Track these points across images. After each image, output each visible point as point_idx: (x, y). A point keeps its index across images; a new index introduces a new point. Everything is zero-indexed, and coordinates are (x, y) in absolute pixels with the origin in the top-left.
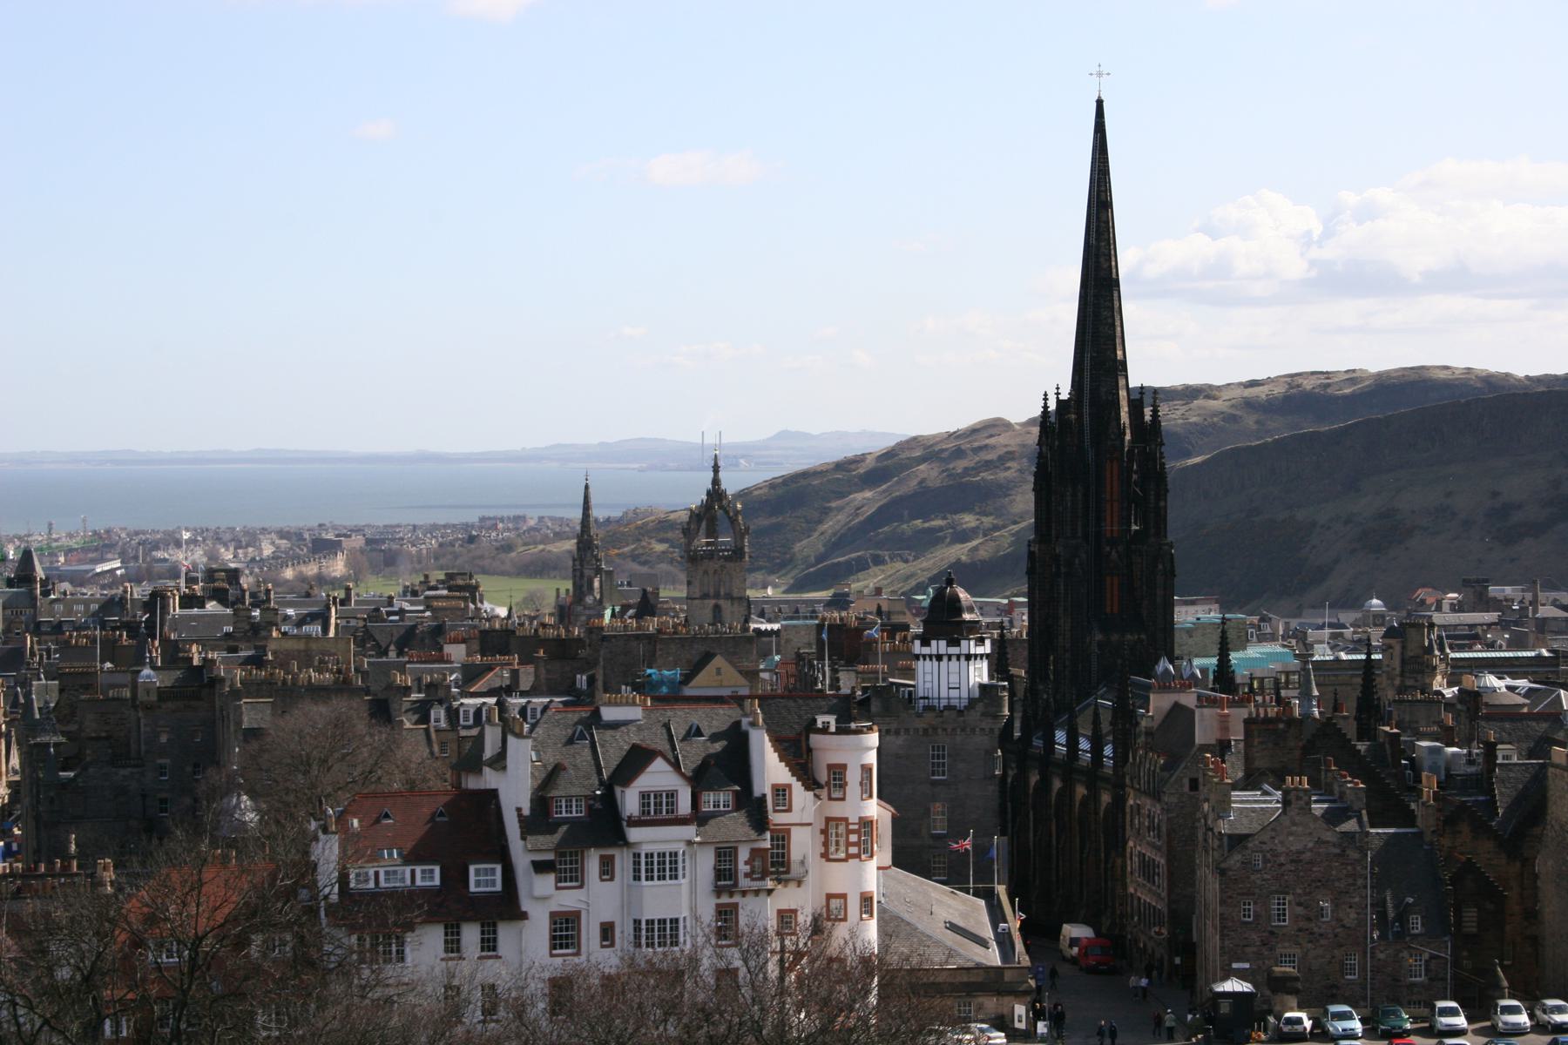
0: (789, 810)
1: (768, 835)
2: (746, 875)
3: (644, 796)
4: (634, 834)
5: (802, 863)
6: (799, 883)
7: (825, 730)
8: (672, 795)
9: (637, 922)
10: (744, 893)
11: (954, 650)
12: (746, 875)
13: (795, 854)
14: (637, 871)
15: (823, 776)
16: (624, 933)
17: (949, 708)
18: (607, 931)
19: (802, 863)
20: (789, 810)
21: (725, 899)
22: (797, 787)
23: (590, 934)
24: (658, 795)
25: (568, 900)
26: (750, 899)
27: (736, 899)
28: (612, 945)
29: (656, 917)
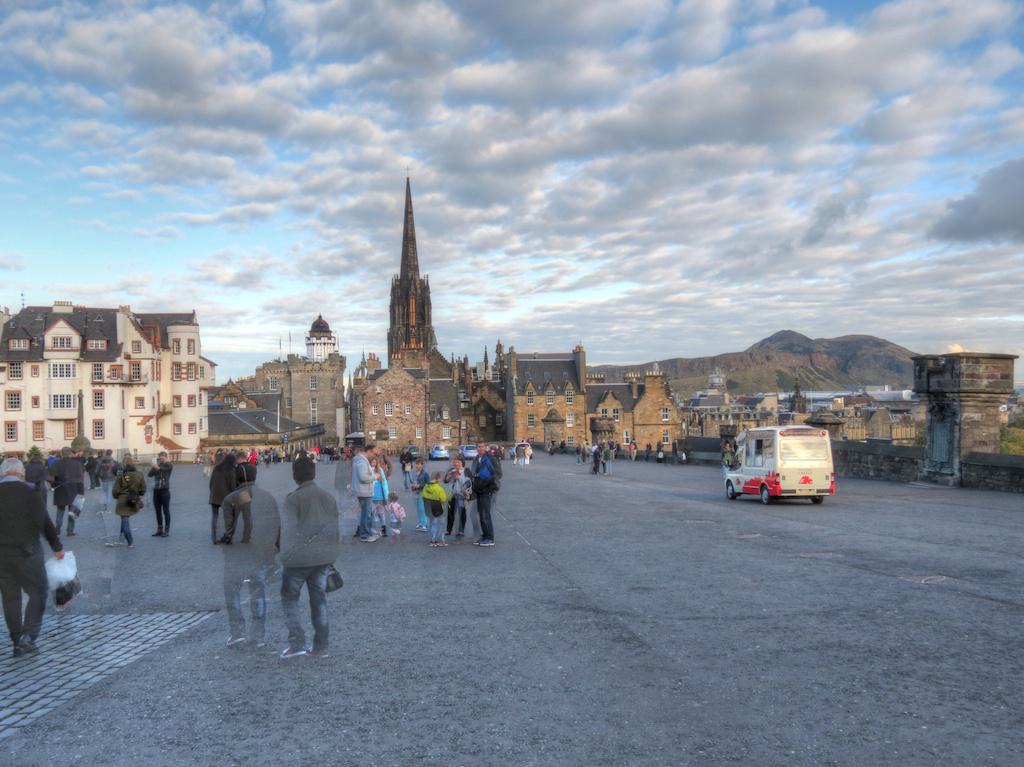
3: (55, 339)
4: (46, 355)
8: (69, 339)
11: (318, 341)
15: (171, 344)
17: (317, 363)
18: (36, 401)
21: (97, 387)
23: (26, 400)
27: (103, 387)
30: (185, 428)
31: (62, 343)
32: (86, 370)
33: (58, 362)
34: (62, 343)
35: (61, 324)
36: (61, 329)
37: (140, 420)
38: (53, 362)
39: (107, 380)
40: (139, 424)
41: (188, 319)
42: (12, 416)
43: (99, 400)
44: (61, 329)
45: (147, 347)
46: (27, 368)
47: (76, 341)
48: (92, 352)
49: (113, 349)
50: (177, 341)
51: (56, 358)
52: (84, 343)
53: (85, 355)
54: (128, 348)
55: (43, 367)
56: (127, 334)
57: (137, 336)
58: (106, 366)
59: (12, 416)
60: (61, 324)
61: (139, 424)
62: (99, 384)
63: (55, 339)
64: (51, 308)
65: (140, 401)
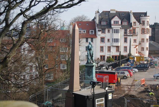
0: (136, 25)
1: (132, 28)
2: (129, 33)
3: (114, 22)
4: (112, 26)
5: (137, 33)
6: (137, 35)
7: (142, 16)
8: (118, 22)
9: (113, 39)
10: (128, 36)
12: (129, 33)
13: (136, 32)
14: (113, 32)
15: (141, 22)
16: (111, 40)
18: (109, 40)
19: (137, 33)
20: (136, 25)
21: (125, 37)
22: (137, 22)
23: (106, 40)
24: (116, 21)
25: (103, 35)
26: (129, 36)
27: (127, 36)
28: (109, 42)
29: (115, 38)
30: (145, 49)
31: (116, 23)
35: (116, 17)
36: (116, 19)
37: (135, 46)
38: (114, 29)
39: (128, 34)
40: (134, 48)
41: (145, 14)
44: (116, 19)
45: (137, 23)
46: (107, 30)
47: (120, 23)
48: (124, 26)
49: (130, 25)
50: (144, 22)
53: (123, 27)
54: (133, 25)
55: (111, 30)
56: (133, 20)
57: (135, 20)
58: (128, 30)
59: (102, 44)
60: (116, 17)
61: (134, 48)
62: (126, 36)
64: (109, 12)
65: (135, 41)
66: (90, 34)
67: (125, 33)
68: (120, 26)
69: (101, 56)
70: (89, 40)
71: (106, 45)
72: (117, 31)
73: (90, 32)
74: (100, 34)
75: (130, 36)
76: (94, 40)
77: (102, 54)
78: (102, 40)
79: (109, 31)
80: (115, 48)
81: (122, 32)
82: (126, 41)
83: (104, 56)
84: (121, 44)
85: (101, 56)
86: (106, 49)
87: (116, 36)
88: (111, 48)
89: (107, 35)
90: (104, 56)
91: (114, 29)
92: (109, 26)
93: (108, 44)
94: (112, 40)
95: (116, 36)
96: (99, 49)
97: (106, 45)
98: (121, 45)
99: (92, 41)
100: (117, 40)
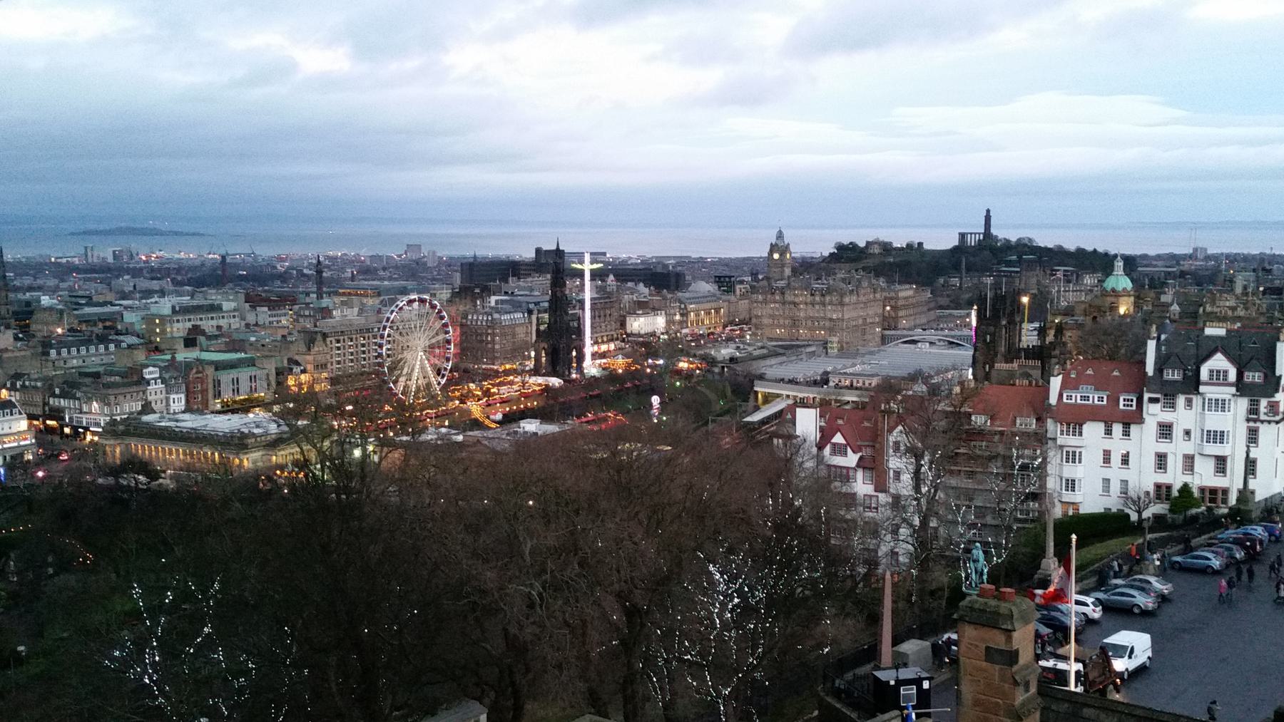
3: (1211, 371)
4: (1202, 389)
8: (1226, 372)
10: (1262, 422)
18: (1188, 433)
21: (1252, 424)
23: (1178, 432)
24: (1218, 372)
25: (1167, 417)
27: (1258, 424)
31: (1218, 378)
32: (1243, 404)
33: (1214, 396)
34: (1218, 378)
35: (1219, 356)
36: (1219, 362)
38: (1208, 396)
39: (1263, 417)
42: (1163, 447)
43: (1253, 436)
44: (1219, 362)
46: (1181, 400)
47: (1232, 376)
51: (1208, 391)
52: (1240, 375)
53: (1242, 388)
55: (1197, 401)
58: (1264, 403)
59: (1163, 447)
60: (1219, 356)
62: (1255, 421)
63: (1211, 371)
66: (1121, 407)
67: (1253, 410)
68: (1233, 390)
69: (1158, 487)
70: (1117, 429)
71: (1177, 449)
72: (1221, 405)
73: (1122, 402)
74: (1154, 413)
75: (1269, 422)
76: (1134, 428)
77: (1163, 479)
78: (1165, 431)
79: (1189, 403)
80: (1211, 464)
81: (1243, 404)
82: (1253, 436)
83: (1169, 487)
84: (1235, 449)
85: (1158, 487)
86: (1175, 464)
87: (1215, 421)
88: (1197, 460)
89: (1183, 415)
90: (1169, 487)
91: (1208, 396)
92: (1192, 384)
93: (1189, 448)
94: (1199, 435)
95: (1215, 421)
96: (1151, 461)
97: (1177, 449)
98: (1233, 453)
99: (1126, 433)
100: (1217, 437)
